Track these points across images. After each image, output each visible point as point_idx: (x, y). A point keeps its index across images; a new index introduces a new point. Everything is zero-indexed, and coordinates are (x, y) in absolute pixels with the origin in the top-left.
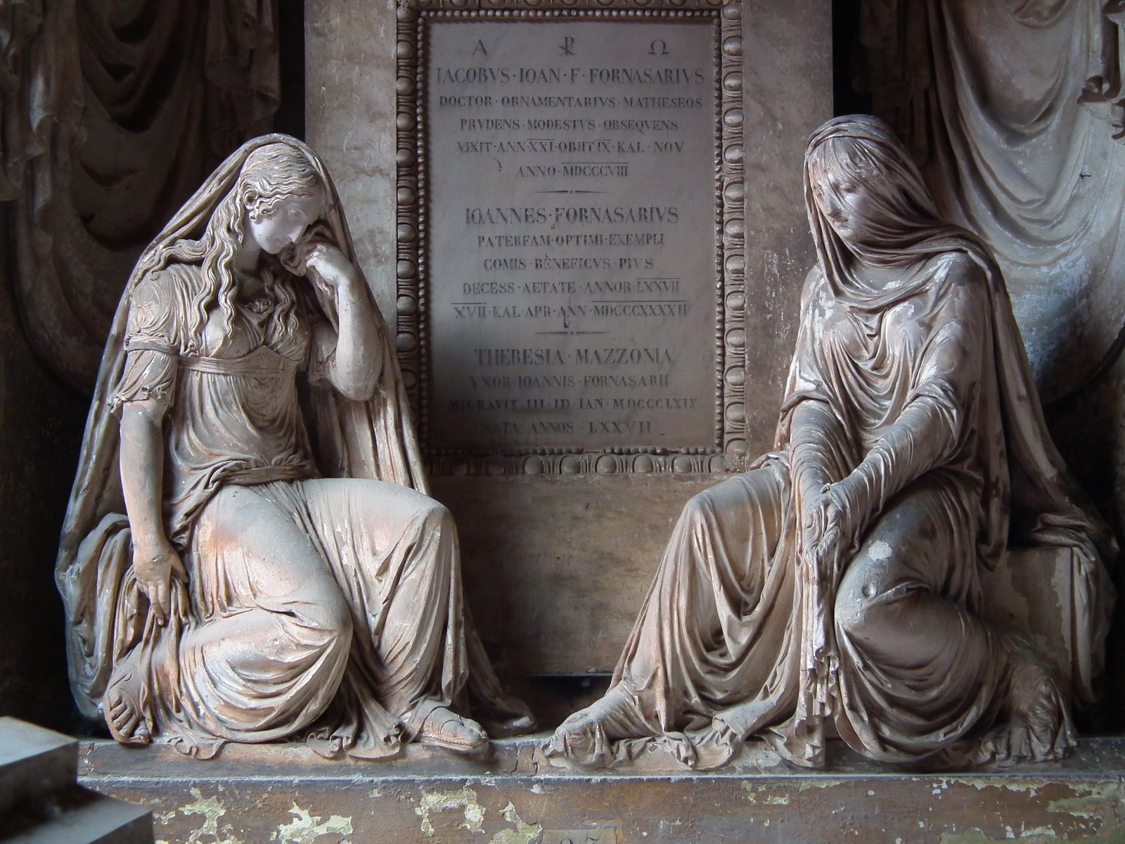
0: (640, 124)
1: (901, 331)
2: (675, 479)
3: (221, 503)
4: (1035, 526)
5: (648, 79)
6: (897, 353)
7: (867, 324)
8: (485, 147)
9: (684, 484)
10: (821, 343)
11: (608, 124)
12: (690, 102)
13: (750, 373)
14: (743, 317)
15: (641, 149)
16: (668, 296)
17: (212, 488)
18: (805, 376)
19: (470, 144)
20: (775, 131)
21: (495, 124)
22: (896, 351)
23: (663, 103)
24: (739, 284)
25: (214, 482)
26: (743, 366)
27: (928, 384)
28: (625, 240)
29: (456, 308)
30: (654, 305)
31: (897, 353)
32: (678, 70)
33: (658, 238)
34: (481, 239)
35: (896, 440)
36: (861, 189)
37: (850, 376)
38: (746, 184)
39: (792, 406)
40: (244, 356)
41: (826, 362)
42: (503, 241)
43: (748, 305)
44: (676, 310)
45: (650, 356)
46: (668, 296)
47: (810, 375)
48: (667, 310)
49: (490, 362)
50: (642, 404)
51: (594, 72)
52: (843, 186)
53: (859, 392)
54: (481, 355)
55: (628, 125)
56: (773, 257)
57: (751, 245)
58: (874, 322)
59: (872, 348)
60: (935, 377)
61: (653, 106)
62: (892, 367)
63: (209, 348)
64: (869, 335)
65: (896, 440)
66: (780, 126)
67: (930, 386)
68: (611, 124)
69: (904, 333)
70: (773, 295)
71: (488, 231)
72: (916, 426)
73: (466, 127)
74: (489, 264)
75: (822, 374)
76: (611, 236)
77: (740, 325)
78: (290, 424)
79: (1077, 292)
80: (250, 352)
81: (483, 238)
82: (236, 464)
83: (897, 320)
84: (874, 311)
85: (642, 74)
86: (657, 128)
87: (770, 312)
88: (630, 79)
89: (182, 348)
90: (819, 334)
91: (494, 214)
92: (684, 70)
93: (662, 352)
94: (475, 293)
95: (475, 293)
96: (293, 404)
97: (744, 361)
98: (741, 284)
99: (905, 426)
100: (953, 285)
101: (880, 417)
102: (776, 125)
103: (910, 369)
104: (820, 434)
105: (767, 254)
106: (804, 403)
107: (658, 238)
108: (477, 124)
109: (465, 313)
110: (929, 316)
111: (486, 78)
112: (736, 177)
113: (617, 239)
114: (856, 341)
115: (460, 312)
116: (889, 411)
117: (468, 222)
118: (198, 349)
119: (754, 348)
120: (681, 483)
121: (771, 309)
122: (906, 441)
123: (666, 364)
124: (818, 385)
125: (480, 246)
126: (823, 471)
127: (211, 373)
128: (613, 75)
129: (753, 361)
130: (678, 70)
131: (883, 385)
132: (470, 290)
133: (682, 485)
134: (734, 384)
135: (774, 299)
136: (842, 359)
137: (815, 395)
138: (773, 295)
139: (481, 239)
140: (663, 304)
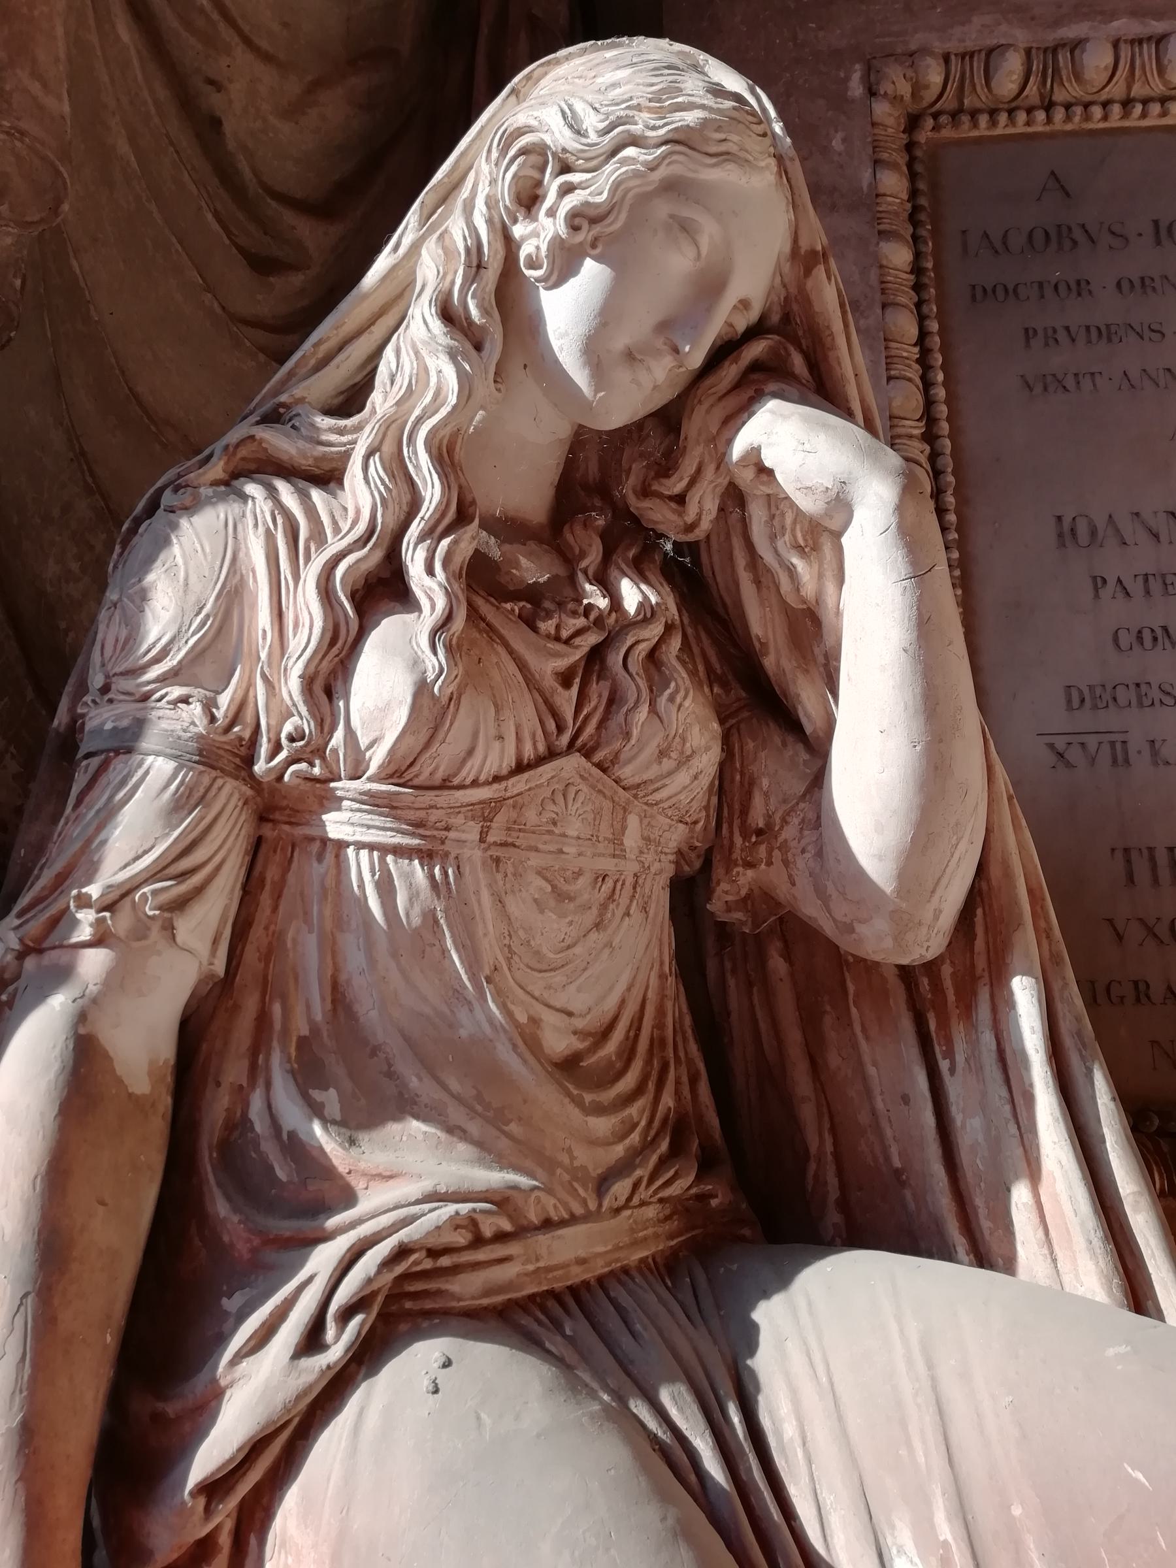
3: (372, 1419)
8: (1087, 384)
17: (338, 1345)
19: (1049, 379)
21: (1107, 334)
25: (346, 1315)
29: (1051, 746)
34: (1099, 582)
40: (497, 779)
42: (1155, 586)
49: (1156, 881)
54: (1128, 861)
63: (363, 742)
71: (1112, 563)
73: (1037, 343)
74: (1125, 639)
78: (658, 1043)
80: (520, 768)
81: (1104, 581)
82: (455, 1223)
89: (264, 748)
91: (1127, 527)
94: (1095, 707)
95: (1095, 707)
96: (662, 977)
108: (1062, 335)
109: (1074, 755)
111: (1075, 243)
115: (1061, 755)
117: (1062, 545)
118: (320, 752)
125: (1097, 596)
127: (371, 847)
132: (1083, 701)
139: (1099, 582)
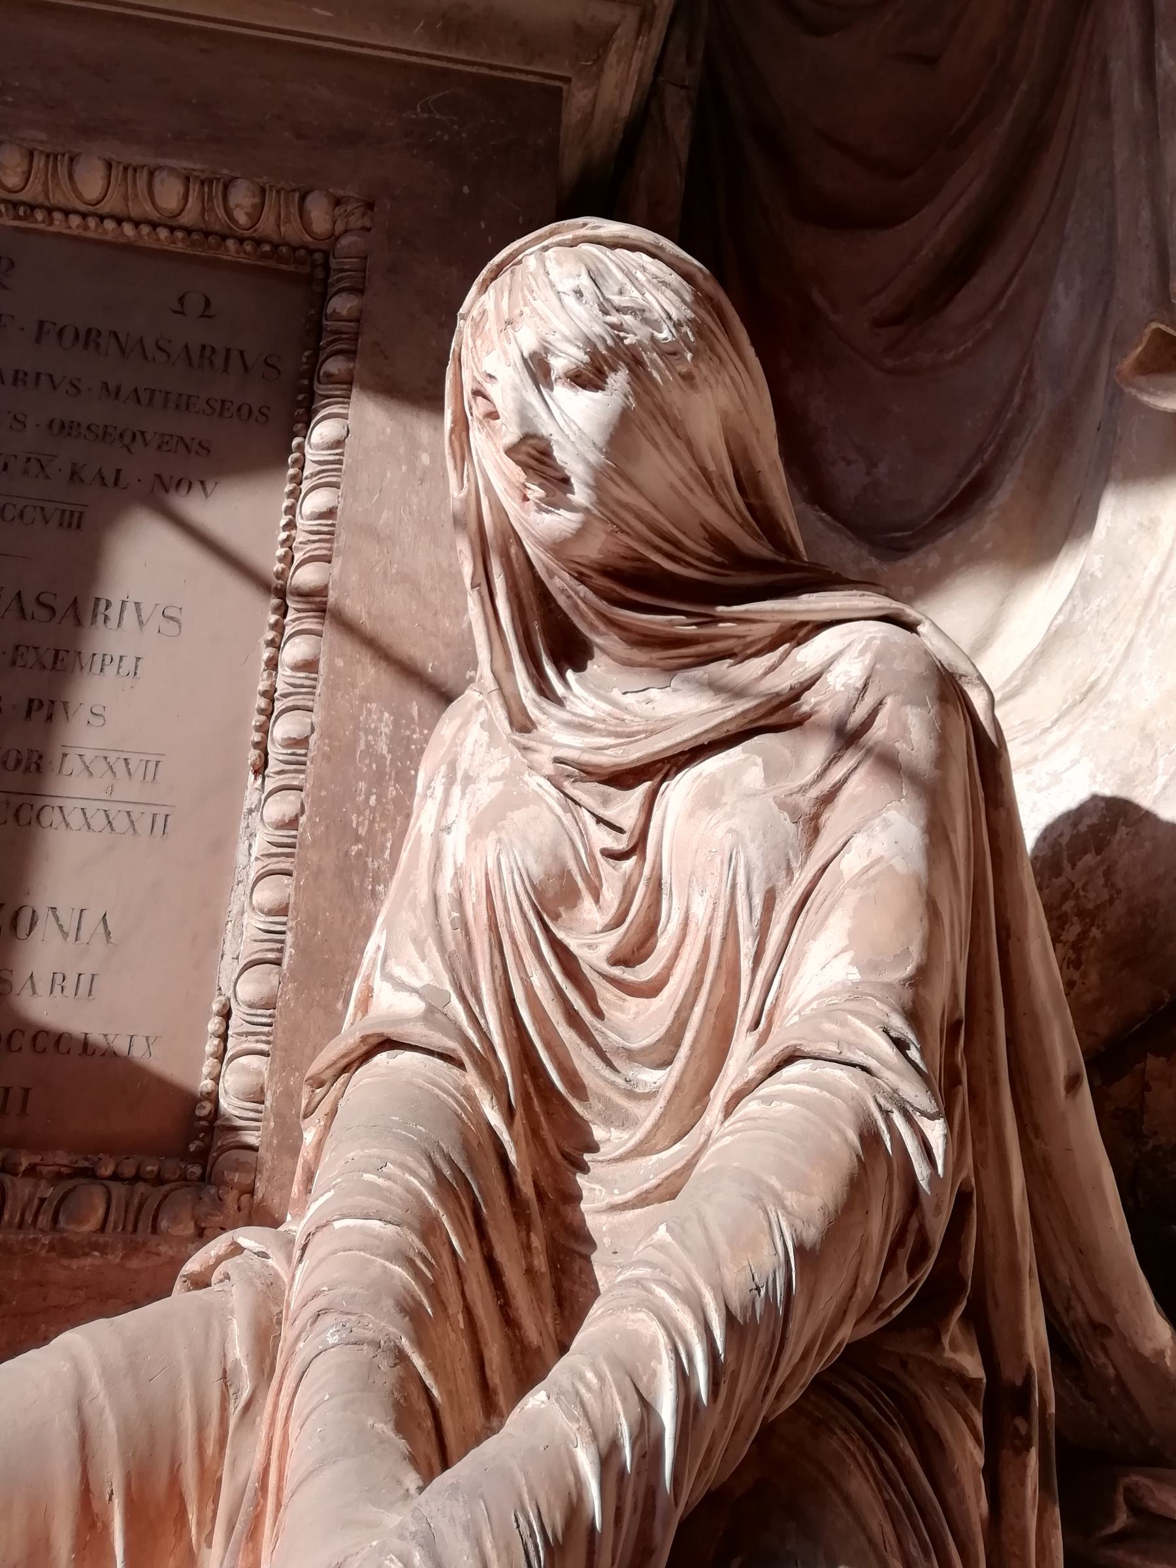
0: (128, 438)
1: (720, 831)
2: (52, 1248)
4: (1111, 1517)
5: (161, 357)
6: (700, 910)
7: (601, 812)
9: (75, 1264)
10: (458, 874)
11: (56, 426)
12: (245, 410)
13: (293, 978)
14: (293, 846)
15: (122, 483)
16: (128, 790)
18: (398, 971)
20: (412, 468)
22: (693, 908)
23: (185, 404)
24: (296, 771)
26: (277, 963)
27: (829, 1013)
28: (49, 662)
30: (91, 807)
31: (700, 910)
32: (228, 351)
33: (128, 665)
35: (723, 1248)
36: (618, 380)
37: (538, 980)
38: (337, 562)
39: (345, 1069)
41: (467, 933)
43: (310, 818)
44: (144, 824)
45: (61, 926)
46: (128, 790)
47: (415, 971)
48: (121, 823)
50: (17, 1041)
51: (47, 326)
52: (558, 365)
53: (566, 1033)
55: (104, 434)
56: (380, 720)
57: (333, 687)
58: (626, 806)
59: (611, 896)
60: (855, 993)
61: (165, 406)
62: (676, 956)
64: (609, 854)
65: (723, 1248)
66: (425, 459)
67: (844, 1024)
68: (66, 428)
69: (729, 840)
70: (373, 800)
72: (802, 1186)
75: (452, 970)
76: (17, 648)
77: (285, 865)
79: (1064, 841)
83: (710, 799)
84: (623, 778)
85: (149, 344)
86: (165, 448)
87: (358, 839)
88: (123, 351)
90: (455, 845)
92: (242, 353)
93: (91, 920)
97: (281, 950)
98: (302, 772)
99: (758, 1182)
100: (889, 701)
101: (625, 1121)
102: (417, 457)
103: (746, 965)
104: (421, 1183)
105: (369, 711)
106: (382, 1058)
107: (128, 665)
110: (814, 792)
112: (319, 549)
113: (31, 658)
114: (565, 874)
116: (661, 1102)
119: (313, 921)
120: (65, 1262)
121: (362, 831)
122: (767, 1251)
123: (99, 945)
124: (433, 1013)
126: (401, 1357)
128: (88, 338)
129: (303, 951)
130: (228, 351)
131: (635, 1021)
133: (68, 1268)
134: (251, 1006)
135: (373, 810)
136: (516, 925)
137: (418, 1033)
138: (373, 800)
140: (113, 809)
